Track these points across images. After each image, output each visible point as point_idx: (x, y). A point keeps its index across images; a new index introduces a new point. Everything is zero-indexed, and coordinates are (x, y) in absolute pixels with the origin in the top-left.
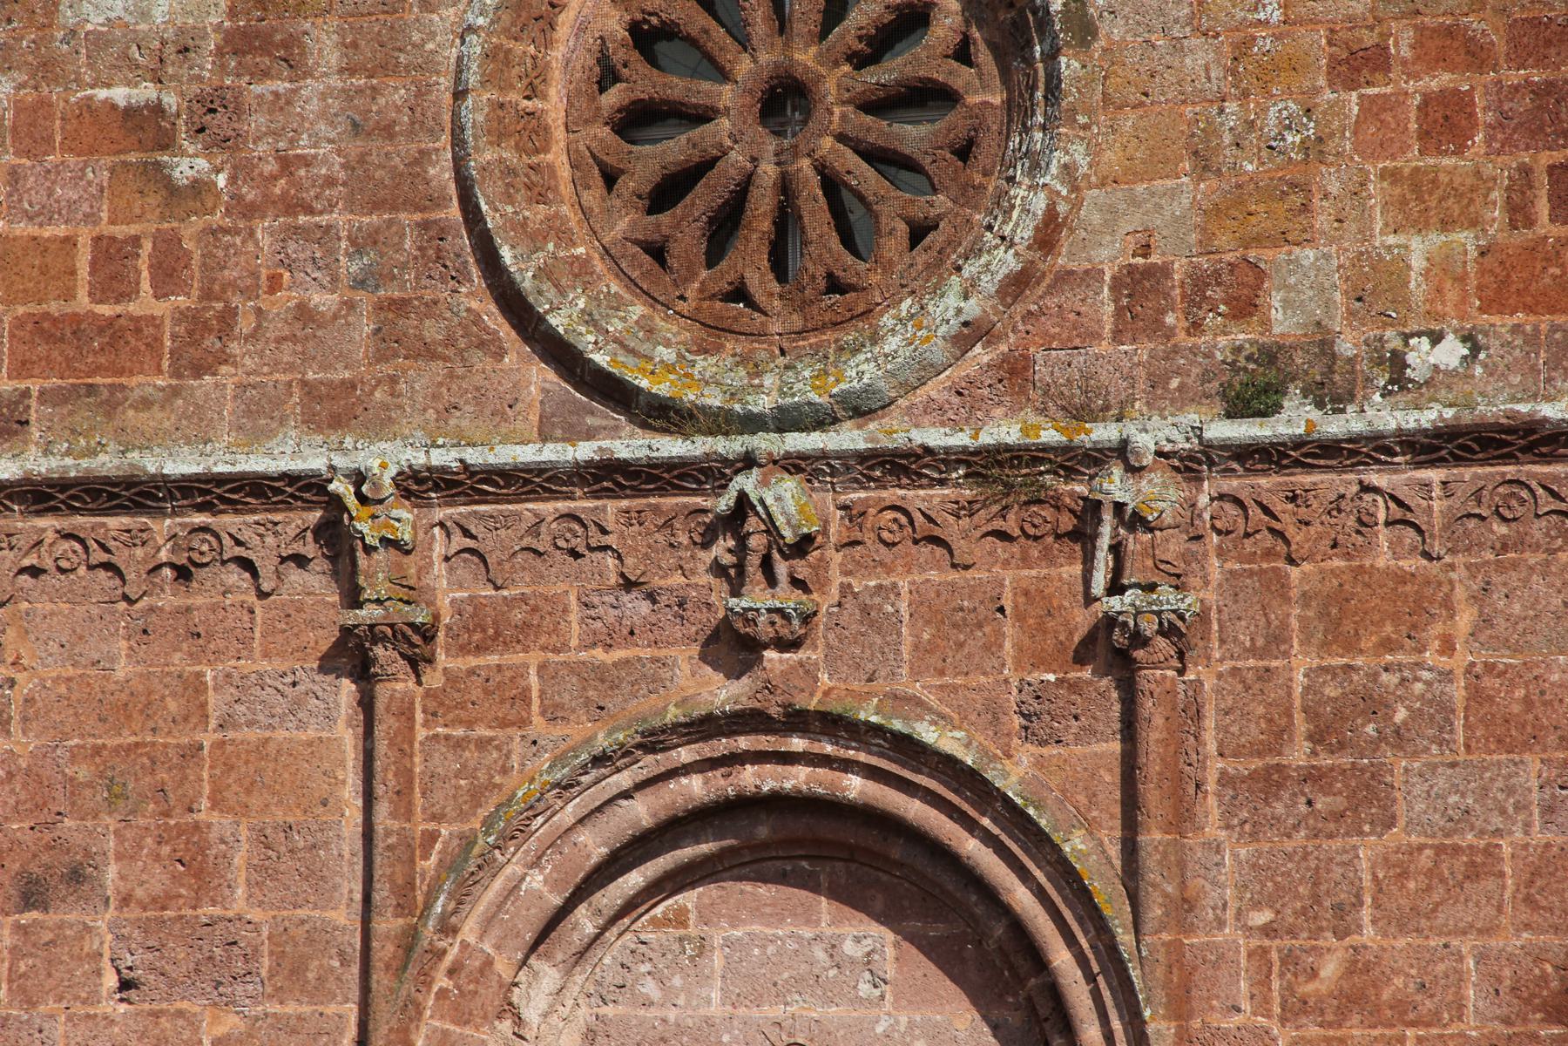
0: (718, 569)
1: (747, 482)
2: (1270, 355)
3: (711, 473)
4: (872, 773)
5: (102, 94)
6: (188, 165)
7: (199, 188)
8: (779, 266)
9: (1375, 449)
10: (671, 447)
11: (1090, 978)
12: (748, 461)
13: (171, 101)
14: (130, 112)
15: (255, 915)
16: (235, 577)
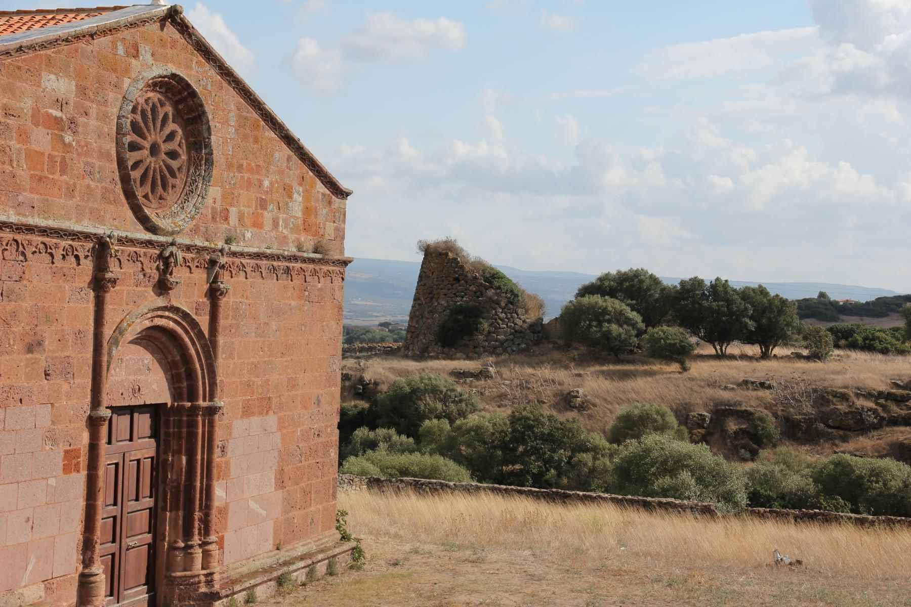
0: (158, 268)
1: (174, 249)
2: (230, 230)
3: (163, 246)
4: (176, 321)
5: (50, 111)
6: (68, 138)
7: (70, 145)
8: (153, 192)
9: (242, 254)
10: (148, 236)
11: (202, 369)
12: (173, 244)
13: (64, 117)
14: (56, 118)
15: (73, 355)
16: (73, 259)
